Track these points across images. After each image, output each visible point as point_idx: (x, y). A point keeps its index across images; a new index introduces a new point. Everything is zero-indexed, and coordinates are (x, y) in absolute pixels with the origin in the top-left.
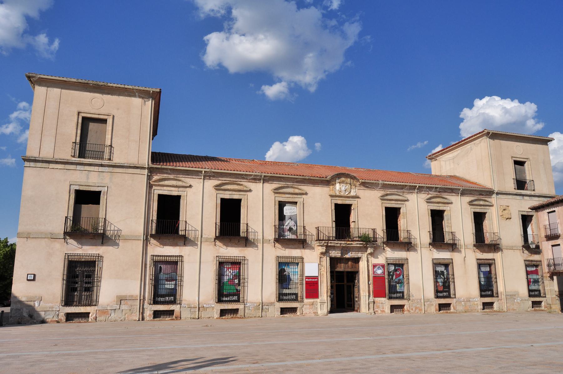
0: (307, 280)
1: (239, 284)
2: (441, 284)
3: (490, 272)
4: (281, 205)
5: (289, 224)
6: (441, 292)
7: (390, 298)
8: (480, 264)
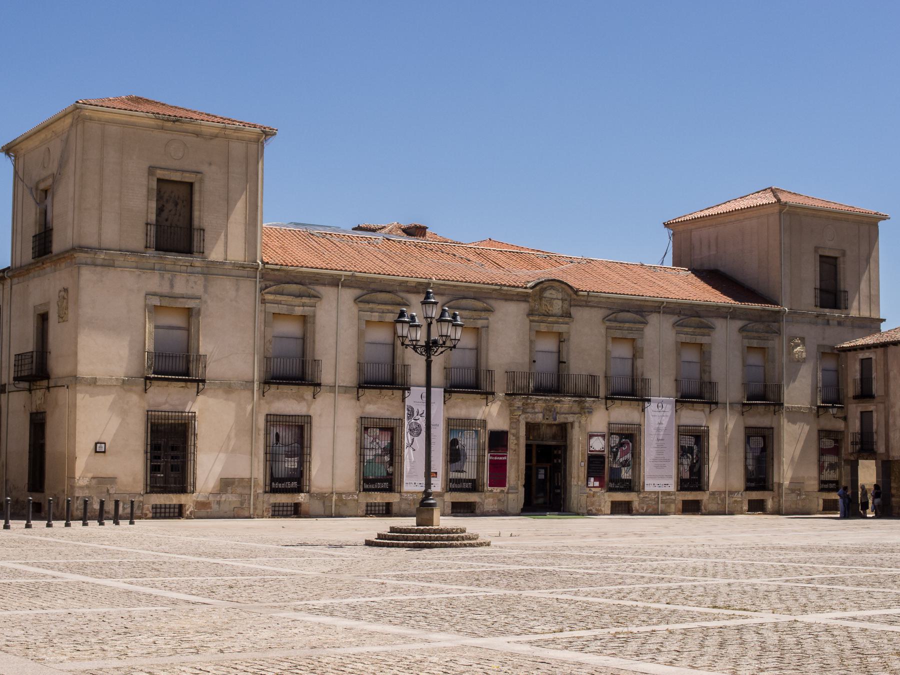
2: (687, 468)
7: (610, 490)
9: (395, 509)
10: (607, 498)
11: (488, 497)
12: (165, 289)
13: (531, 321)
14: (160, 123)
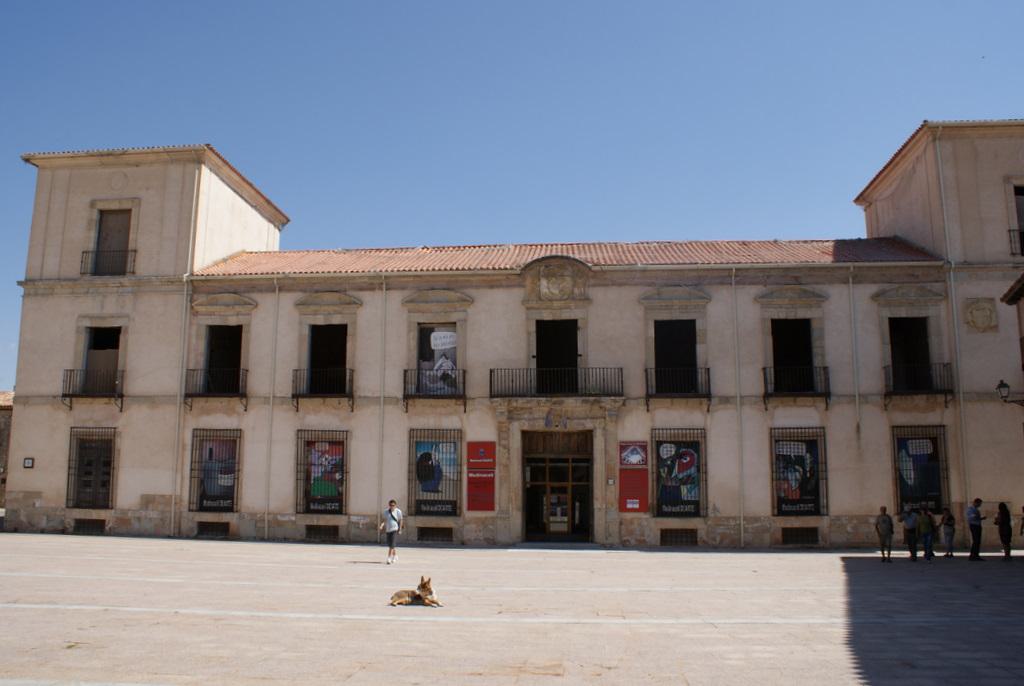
0: (471, 475)
1: (341, 481)
3: (934, 457)
4: (424, 333)
5: (441, 366)
6: (793, 502)
7: (660, 513)
8: (901, 439)
9: (342, 534)
10: (653, 526)
11: (470, 519)
12: (96, 311)
13: (528, 309)
14: (97, 160)
